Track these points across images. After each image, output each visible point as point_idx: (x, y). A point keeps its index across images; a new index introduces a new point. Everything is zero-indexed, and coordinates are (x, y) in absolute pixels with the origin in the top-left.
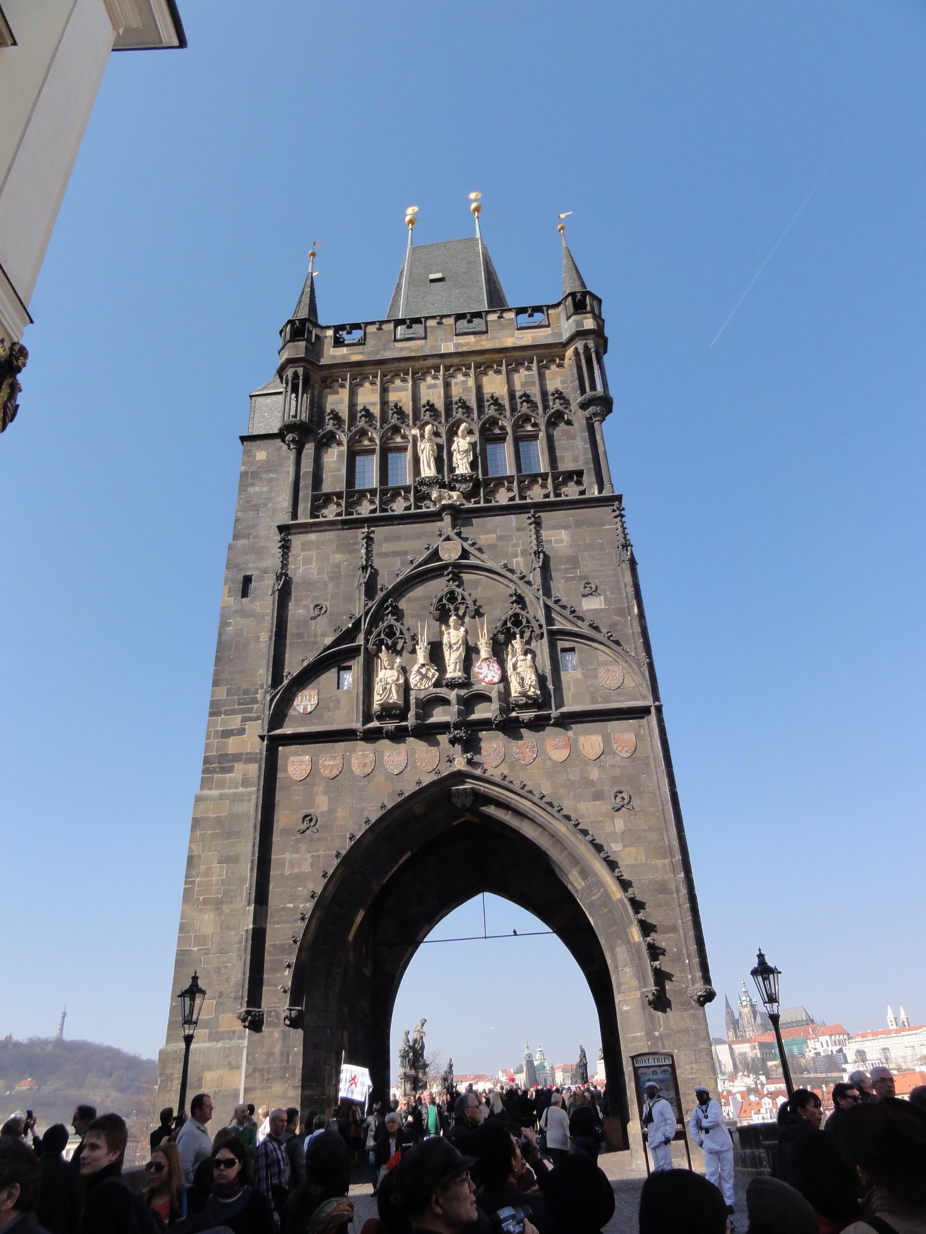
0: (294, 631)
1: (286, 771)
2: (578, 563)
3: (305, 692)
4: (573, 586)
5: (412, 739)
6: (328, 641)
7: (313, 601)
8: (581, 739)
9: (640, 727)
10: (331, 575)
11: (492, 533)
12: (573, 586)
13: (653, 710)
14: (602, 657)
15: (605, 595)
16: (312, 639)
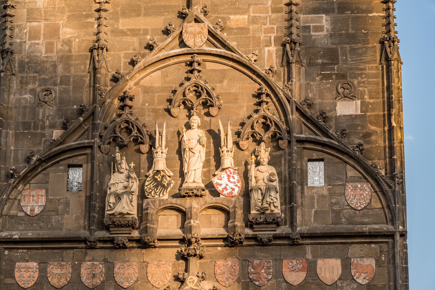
0: (20, 119)
1: (14, 277)
2: (337, 59)
3: (33, 193)
4: (328, 86)
5: (144, 251)
6: (57, 134)
7: (40, 85)
8: (320, 262)
9: (381, 252)
10: (60, 54)
11: (243, 13)
12: (328, 86)
13: (398, 237)
14: (351, 173)
15: (362, 98)
16: (39, 131)
